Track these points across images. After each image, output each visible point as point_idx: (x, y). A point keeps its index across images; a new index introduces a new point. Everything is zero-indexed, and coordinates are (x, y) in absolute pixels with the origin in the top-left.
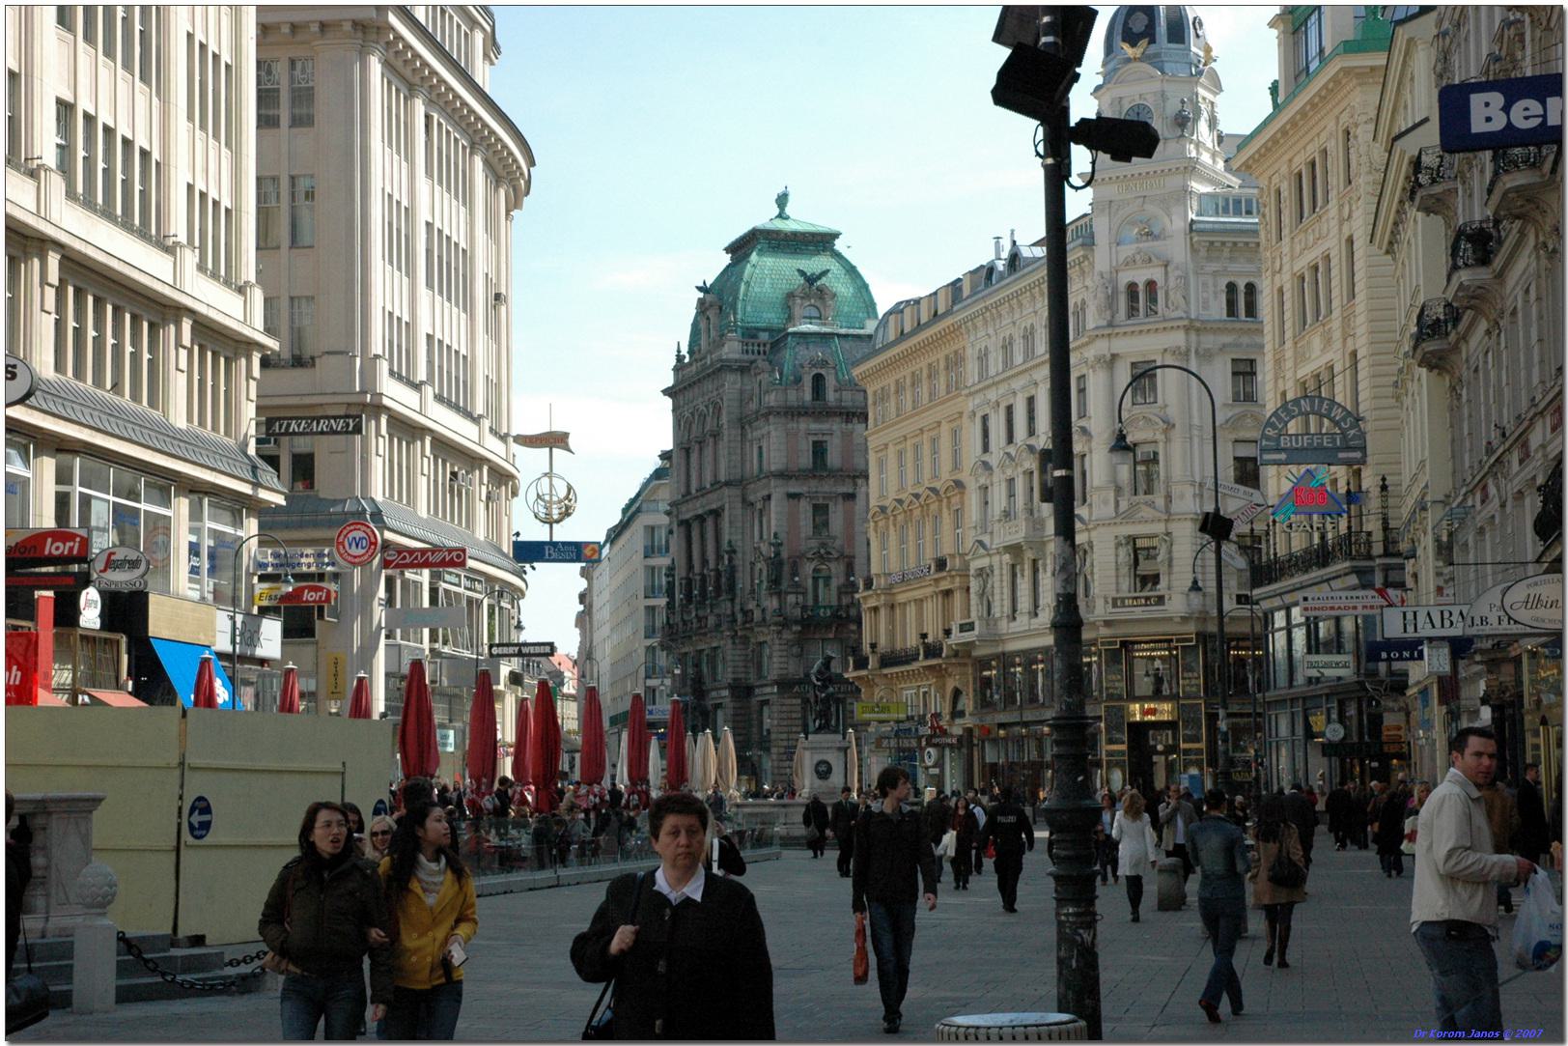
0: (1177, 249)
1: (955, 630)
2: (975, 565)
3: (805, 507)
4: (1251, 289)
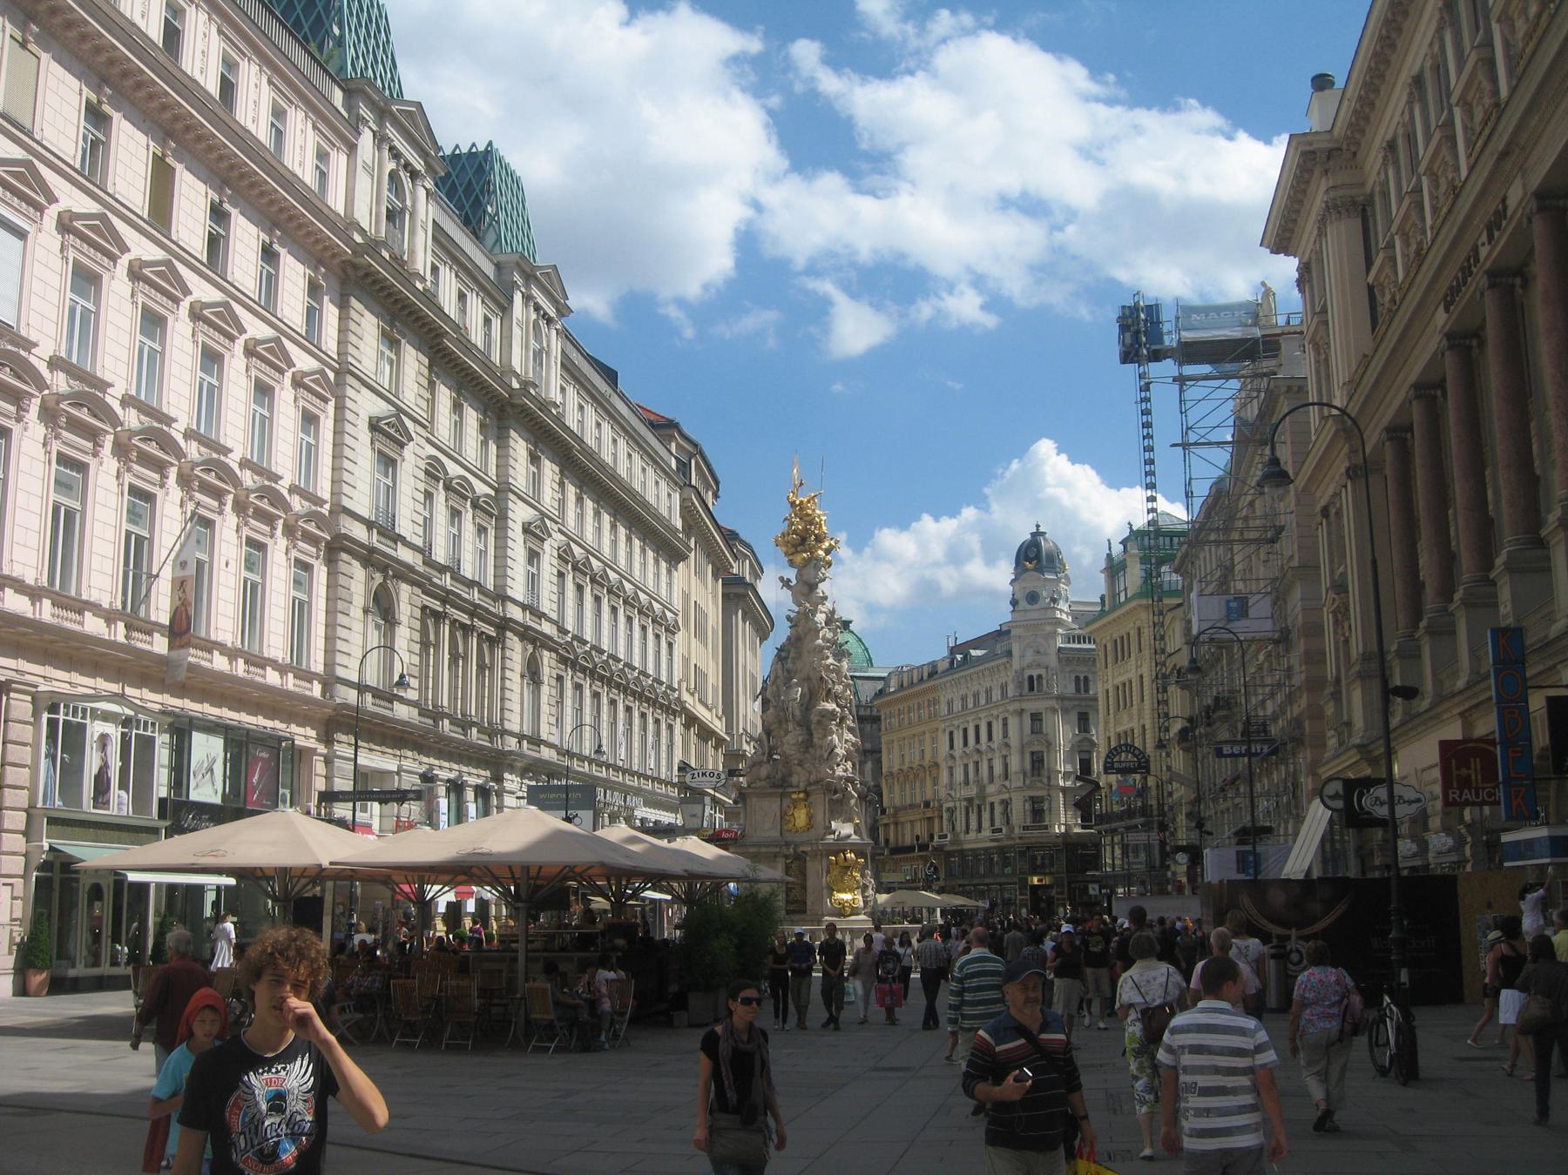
0: (1052, 661)
2: (946, 806)
4: (1086, 678)
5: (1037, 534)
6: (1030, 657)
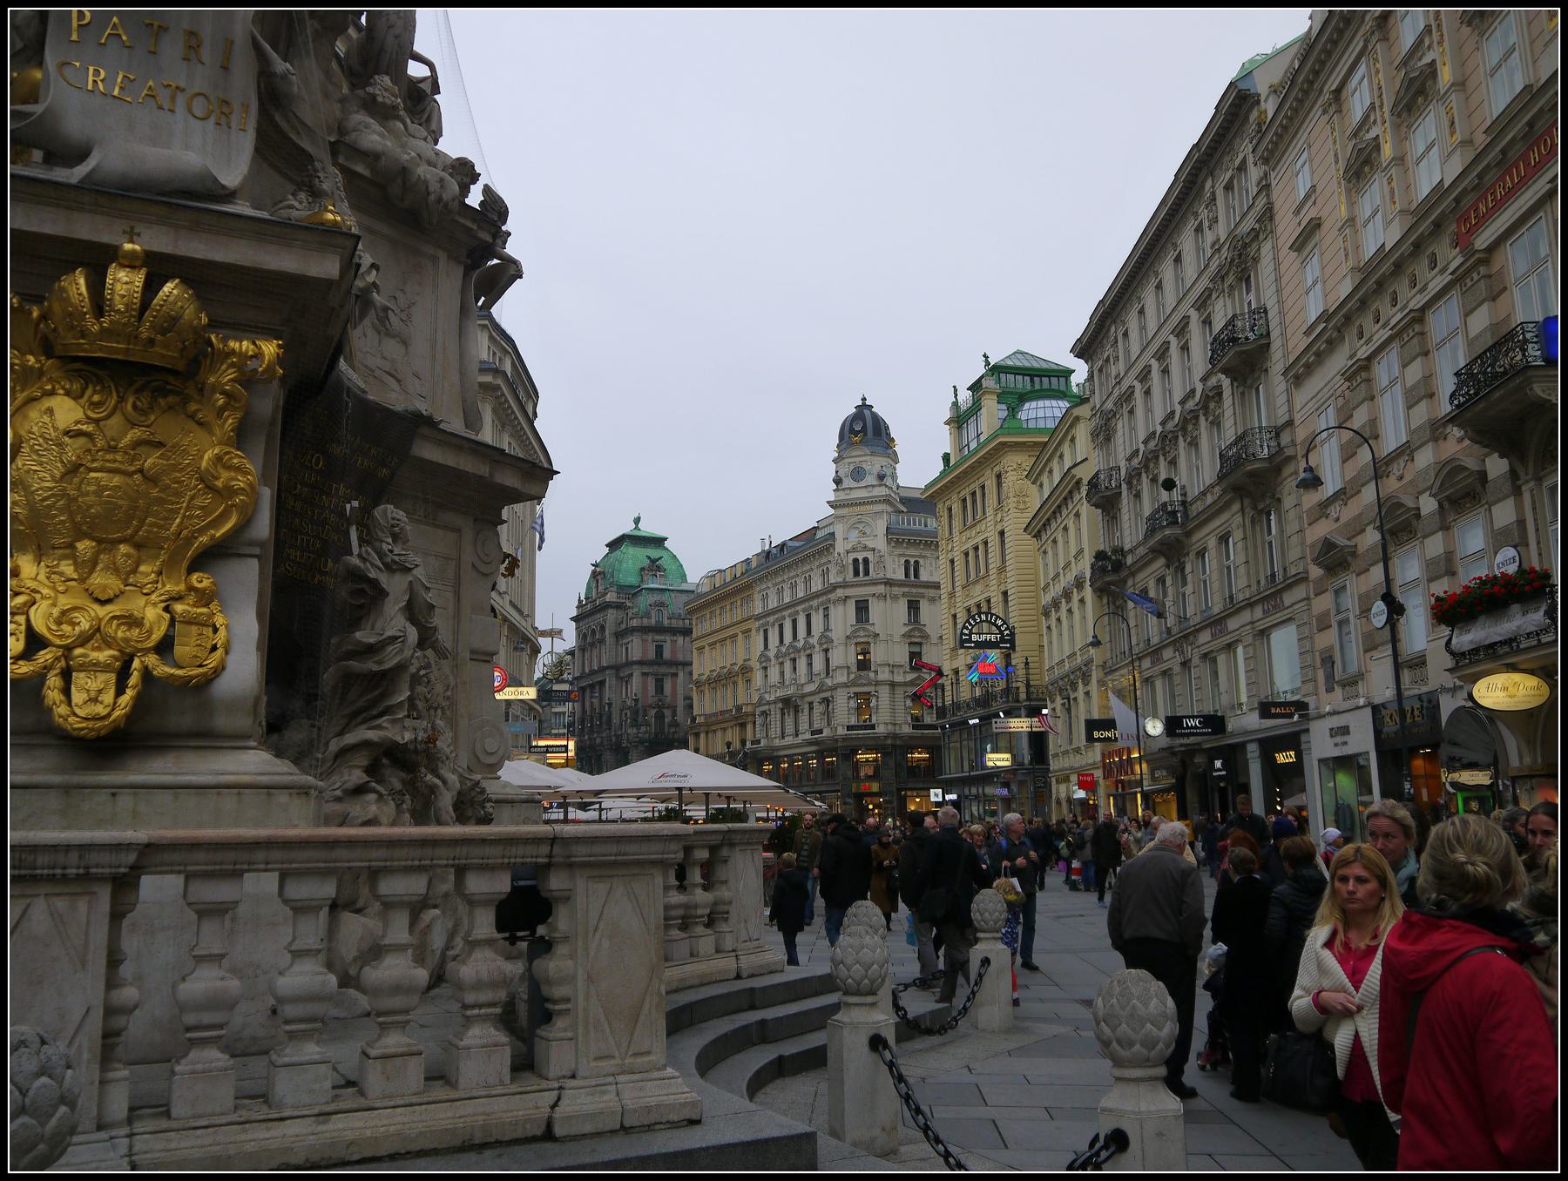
0: (880, 543)
1: (748, 745)
3: (651, 682)
4: (916, 562)
5: (864, 407)
6: (854, 536)
